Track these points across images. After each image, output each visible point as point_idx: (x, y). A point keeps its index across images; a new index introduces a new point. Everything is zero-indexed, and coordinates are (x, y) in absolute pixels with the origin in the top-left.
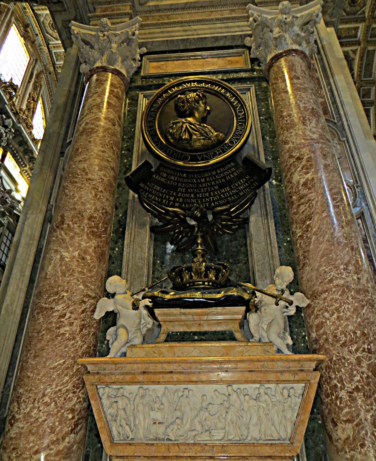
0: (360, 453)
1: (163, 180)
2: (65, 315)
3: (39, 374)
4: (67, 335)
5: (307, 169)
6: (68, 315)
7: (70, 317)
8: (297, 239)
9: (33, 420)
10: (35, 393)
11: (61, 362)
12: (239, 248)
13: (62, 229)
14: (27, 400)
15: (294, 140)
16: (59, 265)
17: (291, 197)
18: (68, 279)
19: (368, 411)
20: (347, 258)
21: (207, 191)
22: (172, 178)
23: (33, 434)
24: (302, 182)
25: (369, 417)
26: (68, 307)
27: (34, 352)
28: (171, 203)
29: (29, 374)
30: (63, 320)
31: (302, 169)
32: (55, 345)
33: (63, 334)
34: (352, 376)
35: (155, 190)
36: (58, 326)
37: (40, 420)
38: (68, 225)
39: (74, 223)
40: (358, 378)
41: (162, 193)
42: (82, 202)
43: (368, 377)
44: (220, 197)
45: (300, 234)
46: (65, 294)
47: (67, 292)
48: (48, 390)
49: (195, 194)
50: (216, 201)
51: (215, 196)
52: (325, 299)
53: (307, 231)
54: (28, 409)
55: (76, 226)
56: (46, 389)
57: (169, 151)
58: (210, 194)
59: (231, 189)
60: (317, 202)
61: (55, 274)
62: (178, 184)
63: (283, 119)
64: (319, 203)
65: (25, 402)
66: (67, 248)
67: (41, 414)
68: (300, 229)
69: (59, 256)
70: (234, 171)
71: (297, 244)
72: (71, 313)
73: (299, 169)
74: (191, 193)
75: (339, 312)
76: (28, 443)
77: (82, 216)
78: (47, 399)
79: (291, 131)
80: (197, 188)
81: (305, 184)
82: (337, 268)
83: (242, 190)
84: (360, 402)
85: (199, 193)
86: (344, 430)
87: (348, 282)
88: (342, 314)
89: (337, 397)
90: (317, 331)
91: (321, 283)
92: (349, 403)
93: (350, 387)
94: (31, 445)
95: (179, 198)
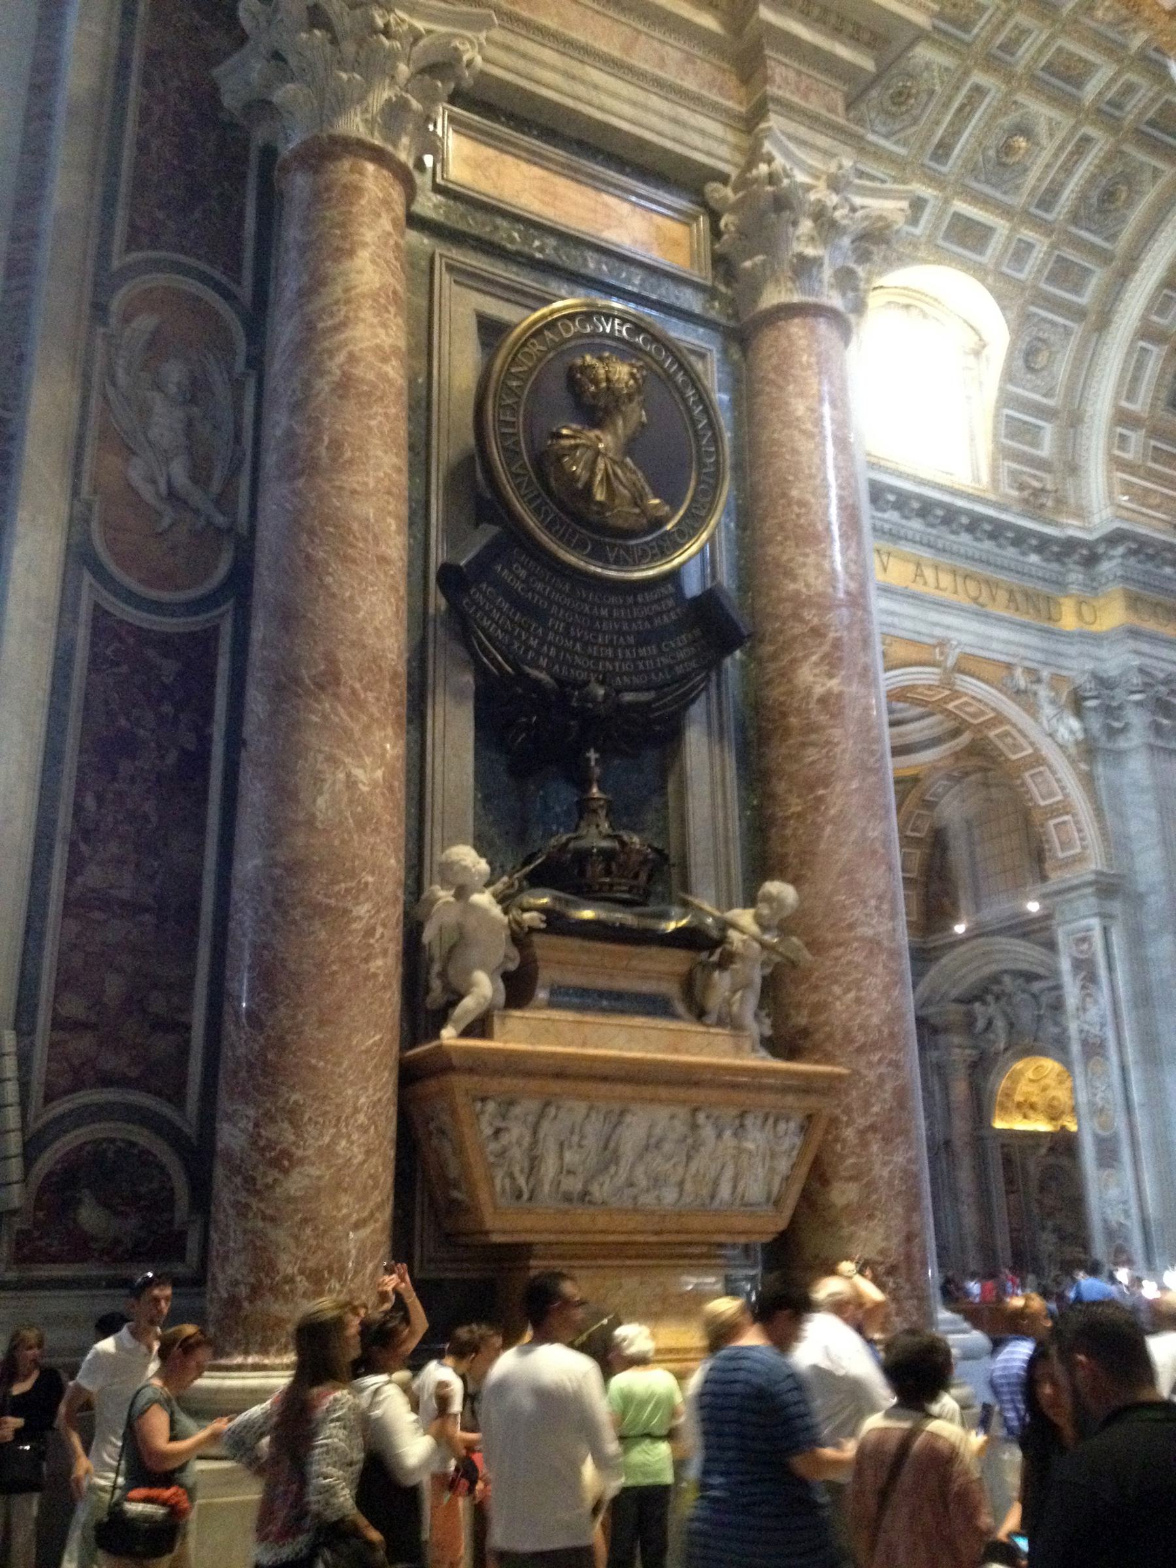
0: (866, 1228)
1: (519, 586)
2: (374, 929)
3: (339, 1064)
4: (381, 978)
5: (832, 665)
6: (379, 931)
7: (382, 936)
8: (787, 818)
9: (340, 1161)
10: (337, 1106)
11: (377, 1037)
12: (645, 793)
13: (336, 696)
14: (321, 1120)
15: (812, 580)
16: (345, 799)
17: (784, 715)
18: (372, 840)
19: (885, 1164)
20: (882, 886)
21: (611, 641)
22: (539, 586)
23: (345, 1190)
24: (819, 690)
25: (885, 1173)
26: (378, 912)
27: (315, 1009)
28: (530, 654)
29: (314, 1061)
30: (372, 941)
31: (822, 659)
32: (364, 1000)
33: (375, 975)
34: (867, 1105)
35: (499, 609)
36: (364, 955)
37: (356, 1161)
38: (354, 692)
39: (366, 689)
40: (875, 1109)
41: (512, 621)
42: (376, 629)
43: (891, 1110)
44: (636, 667)
45: (799, 808)
46: (370, 879)
47: (372, 873)
48: (363, 1100)
49: (586, 644)
50: (625, 673)
51: (624, 660)
52: (837, 959)
53: (817, 809)
54: (327, 1139)
55: (371, 696)
56: (358, 1097)
57: (547, 514)
58: (615, 653)
59: (661, 653)
60: (844, 751)
61: (341, 823)
62: (550, 605)
63: (789, 505)
64: (847, 756)
65: (316, 1123)
66: (360, 756)
67: (355, 1149)
68: (799, 796)
69: (341, 776)
70: (673, 609)
71: (784, 827)
72: (384, 925)
73: (814, 658)
74: (576, 640)
75: (859, 989)
76: (339, 1208)
77: (380, 667)
78: (361, 1118)
79: (808, 550)
80: (591, 629)
81: (823, 701)
82: (864, 902)
83: (682, 662)
84: (875, 1148)
85: (593, 644)
86: (843, 1192)
87: (879, 934)
88: (863, 993)
89: (837, 1140)
90: (810, 1015)
91: (833, 925)
92: (858, 1150)
93: (862, 1122)
94: (345, 1211)
95: (550, 644)
